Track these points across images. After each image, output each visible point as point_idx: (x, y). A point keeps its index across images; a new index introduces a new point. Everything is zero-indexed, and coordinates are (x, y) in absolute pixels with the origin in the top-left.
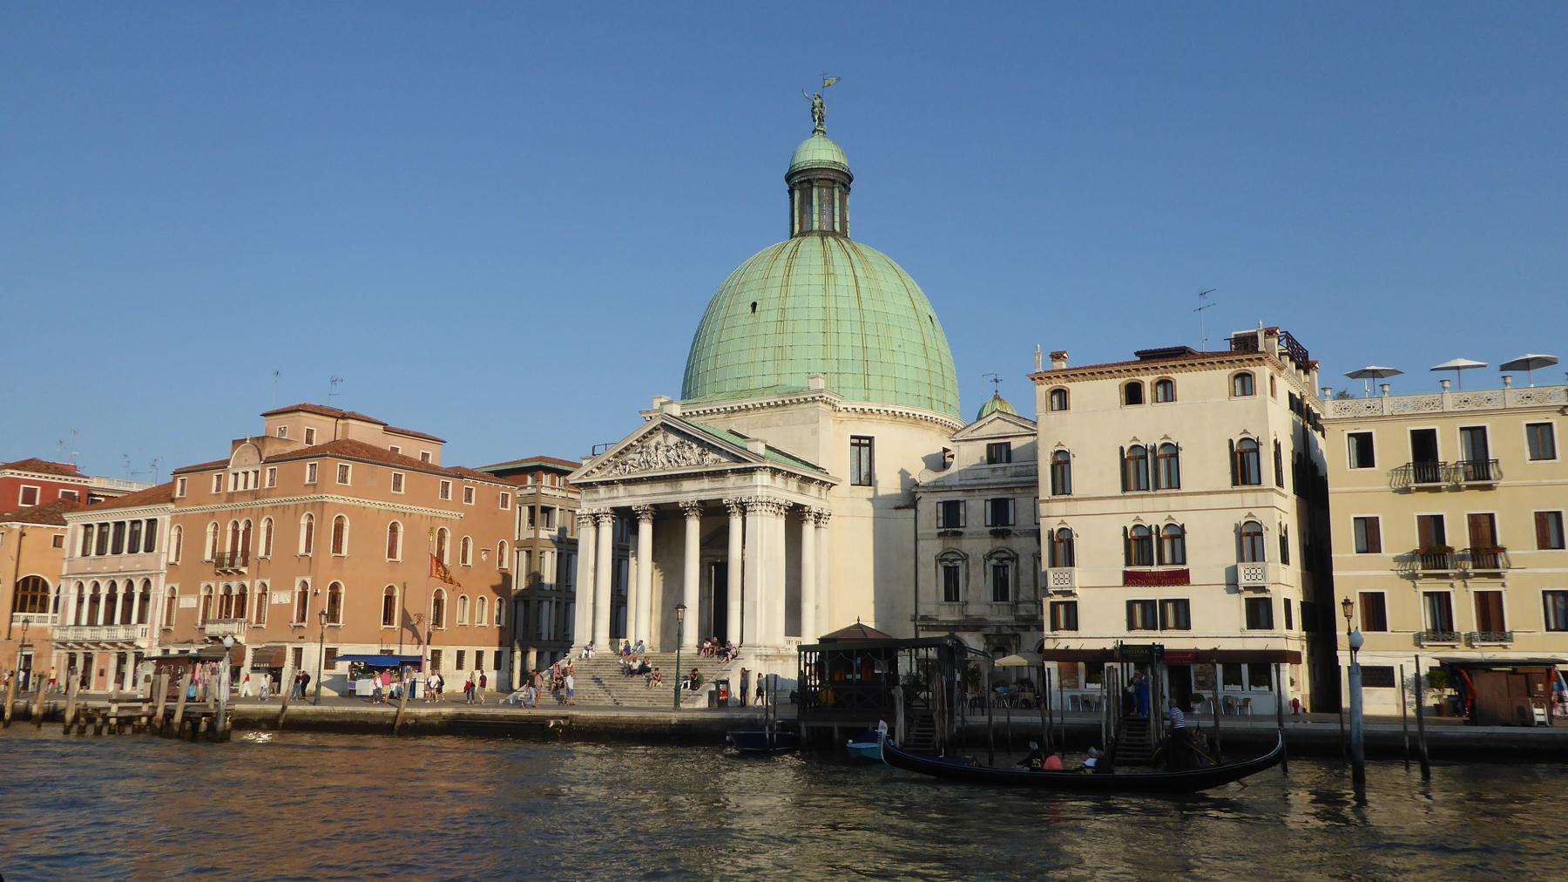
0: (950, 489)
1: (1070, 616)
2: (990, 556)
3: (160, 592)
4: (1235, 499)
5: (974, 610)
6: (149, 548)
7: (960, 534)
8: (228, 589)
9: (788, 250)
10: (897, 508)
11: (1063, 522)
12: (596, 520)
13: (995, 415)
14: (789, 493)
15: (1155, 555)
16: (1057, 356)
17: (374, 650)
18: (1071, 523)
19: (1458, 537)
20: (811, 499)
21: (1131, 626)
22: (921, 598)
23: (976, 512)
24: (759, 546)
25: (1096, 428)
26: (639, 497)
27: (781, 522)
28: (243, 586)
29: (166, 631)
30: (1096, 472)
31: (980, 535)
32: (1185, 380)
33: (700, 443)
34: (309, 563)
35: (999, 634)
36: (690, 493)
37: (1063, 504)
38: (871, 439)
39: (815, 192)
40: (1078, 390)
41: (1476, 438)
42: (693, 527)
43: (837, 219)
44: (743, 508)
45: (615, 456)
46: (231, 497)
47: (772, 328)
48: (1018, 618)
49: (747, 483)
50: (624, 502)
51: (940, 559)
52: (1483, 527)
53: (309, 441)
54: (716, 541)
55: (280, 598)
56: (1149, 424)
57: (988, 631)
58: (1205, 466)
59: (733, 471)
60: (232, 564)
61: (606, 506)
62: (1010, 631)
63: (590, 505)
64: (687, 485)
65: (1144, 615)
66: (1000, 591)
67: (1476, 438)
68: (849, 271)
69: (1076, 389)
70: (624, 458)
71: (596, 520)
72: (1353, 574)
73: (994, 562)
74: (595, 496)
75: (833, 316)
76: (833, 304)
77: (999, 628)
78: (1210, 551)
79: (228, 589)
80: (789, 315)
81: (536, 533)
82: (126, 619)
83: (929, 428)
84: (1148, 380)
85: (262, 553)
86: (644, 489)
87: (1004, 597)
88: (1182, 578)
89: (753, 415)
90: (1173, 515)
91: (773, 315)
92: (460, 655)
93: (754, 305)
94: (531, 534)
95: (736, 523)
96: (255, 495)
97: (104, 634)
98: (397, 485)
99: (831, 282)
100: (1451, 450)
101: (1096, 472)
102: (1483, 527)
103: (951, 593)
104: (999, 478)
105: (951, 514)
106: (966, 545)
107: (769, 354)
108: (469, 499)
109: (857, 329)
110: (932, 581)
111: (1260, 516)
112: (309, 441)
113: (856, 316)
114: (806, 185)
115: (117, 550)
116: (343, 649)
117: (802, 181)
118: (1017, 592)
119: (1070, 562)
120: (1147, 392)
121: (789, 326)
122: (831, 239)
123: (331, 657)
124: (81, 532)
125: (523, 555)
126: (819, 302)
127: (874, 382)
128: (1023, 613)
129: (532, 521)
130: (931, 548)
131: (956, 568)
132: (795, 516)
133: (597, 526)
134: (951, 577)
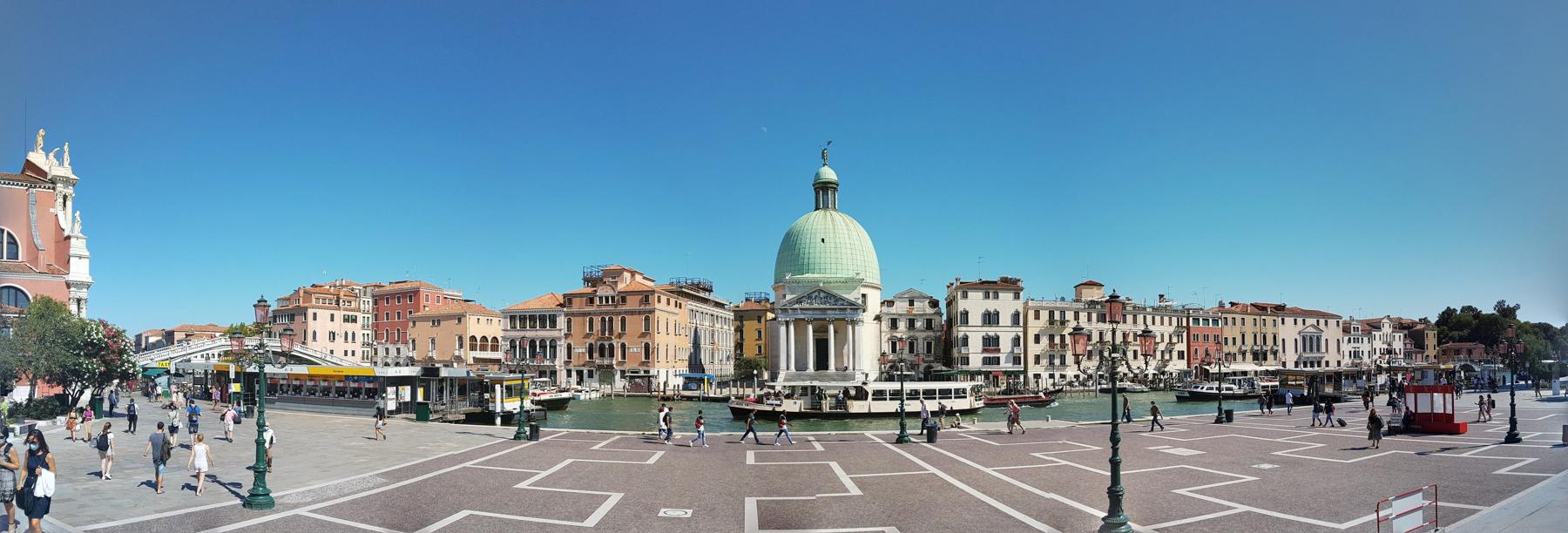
1: (966, 361)
12: (787, 323)
15: (991, 343)
30: (975, 318)
36: (831, 315)
56: (991, 305)
58: (1005, 319)
66: (911, 351)
71: (787, 323)
72: (1034, 349)
78: (1005, 345)
100: (1057, 316)
101: (975, 318)
105: (894, 324)
110: (887, 348)
117: (823, 188)
130: (885, 337)
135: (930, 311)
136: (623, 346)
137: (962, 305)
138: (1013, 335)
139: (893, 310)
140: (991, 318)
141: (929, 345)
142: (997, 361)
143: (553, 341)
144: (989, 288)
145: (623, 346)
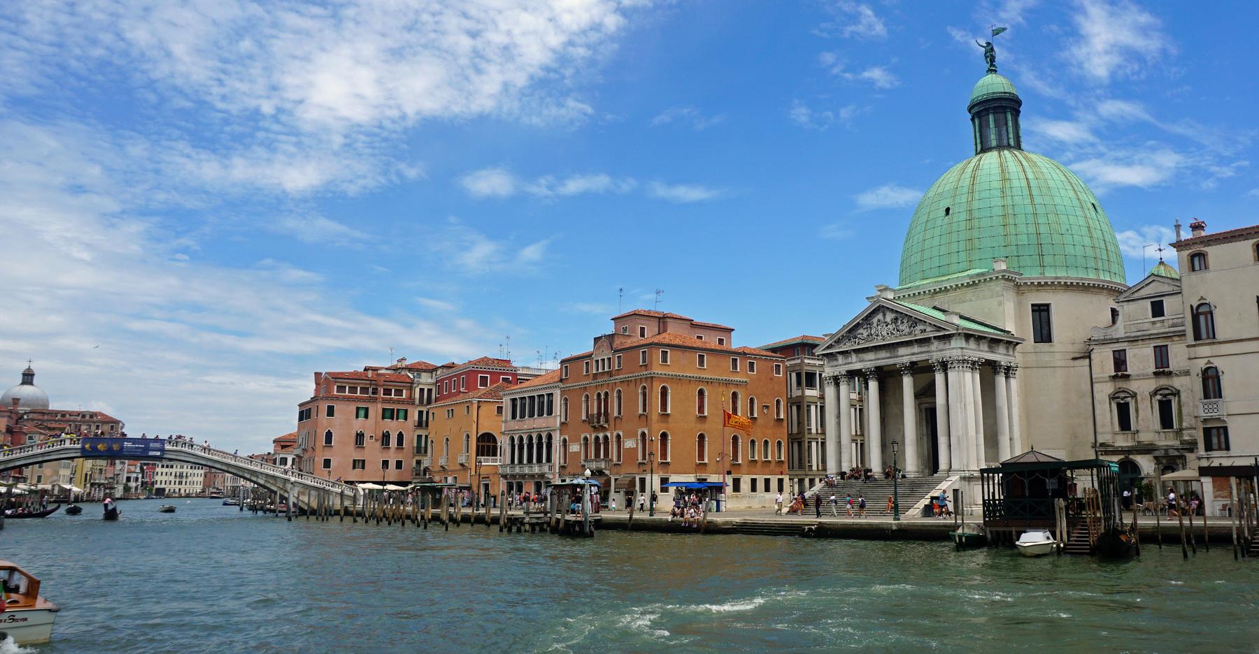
0: (1117, 341)
2: (1155, 393)
3: (557, 439)
5: (1145, 437)
6: (550, 413)
7: (1128, 376)
8: (597, 438)
9: (972, 165)
10: (1074, 359)
11: (1209, 362)
14: (982, 353)
16: (1197, 227)
17: (691, 478)
18: (1217, 362)
20: (1000, 356)
22: (1099, 429)
23: (1141, 359)
24: (961, 390)
27: (977, 376)
28: (606, 438)
29: (562, 467)
31: (1144, 377)
34: (644, 417)
35: (1166, 456)
36: (905, 356)
37: (1207, 348)
38: (1048, 305)
39: (991, 118)
40: (1212, 251)
42: (907, 381)
43: (1011, 136)
44: (944, 366)
45: (850, 331)
46: (595, 376)
49: (947, 346)
51: (1113, 397)
53: (642, 335)
54: (925, 393)
55: (629, 444)
57: (1157, 453)
60: (599, 422)
61: (843, 370)
62: (1176, 453)
64: (902, 351)
66: (1166, 421)
68: (1022, 176)
69: (1212, 251)
71: (836, 380)
73: (1159, 397)
75: (1011, 211)
76: (1010, 202)
77: (1166, 450)
79: (597, 438)
80: (976, 214)
81: (803, 392)
82: (539, 460)
83: (1098, 293)
85: (616, 414)
86: (871, 356)
87: (1172, 427)
89: (952, 294)
91: (963, 216)
92: (754, 481)
93: (948, 210)
94: (799, 393)
95: (939, 378)
96: (610, 374)
97: (527, 470)
98: (701, 363)
99: (1008, 185)
103: (1125, 424)
104: (1158, 329)
106: (1133, 386)
107: (962, 246)
108: (752, 369)
109: (1031, 219)
110: (1108, 416)
112: (642, 335)
113: (1030, 209)
115: (531, 415)
116: (674, 478)
121: (976, 223)
122: (1006, 152)
123: (664, 481)
124: (510, 403)
125: (794, 408)
127: (1048, 260)
128: (1186, 438)
129: (799, 383)
130: (1105, 390)
131: (1127, 404)
132: (989, 370)
133: (837, 385)
134: (1123, 411)
136: (618, 436)
139: (1120, 330)
143: (550, 437)
145: (618, 436)
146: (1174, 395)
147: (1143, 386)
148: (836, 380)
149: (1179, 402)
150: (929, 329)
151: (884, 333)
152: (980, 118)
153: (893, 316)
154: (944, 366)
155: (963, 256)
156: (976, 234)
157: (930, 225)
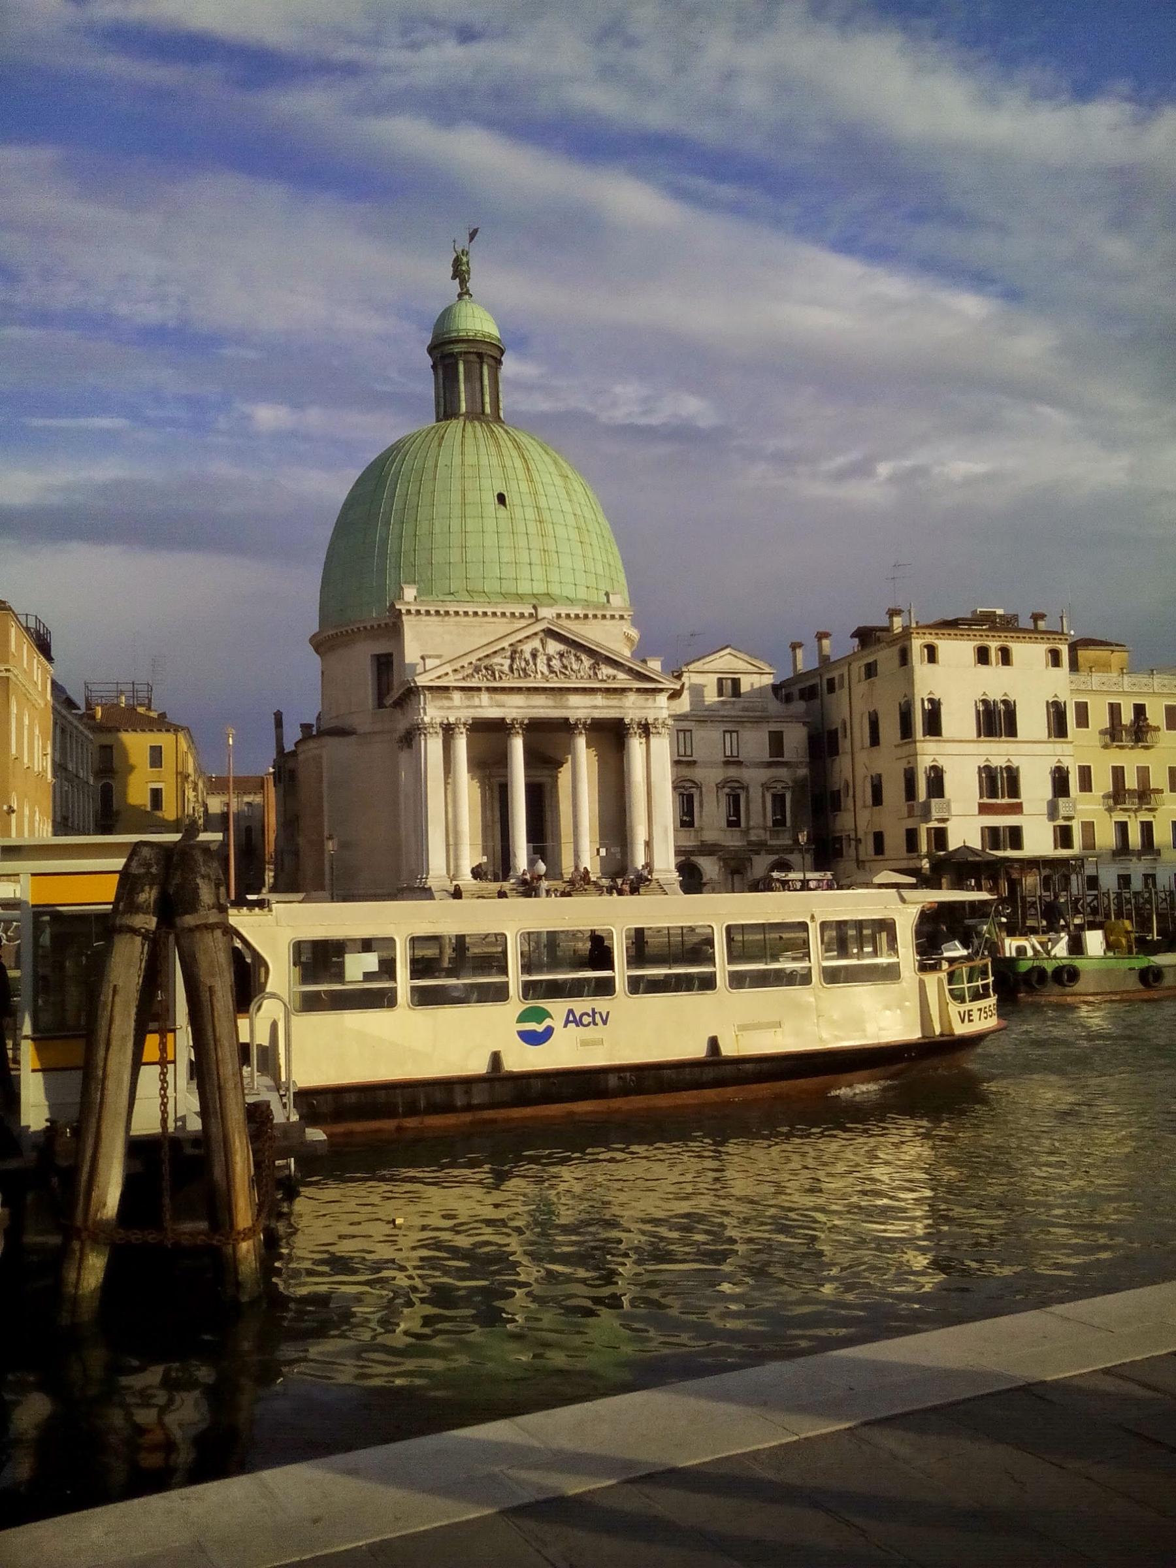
2: (720, 786)
4: (1049, 748)
5: (710, 836)
7: (695, 762)
13: (728, 650)
19: (1131, 782)
21: (1056, 848)
25: (952, 678)
26: (514, 708)
30: (959, 720)
32: (1018, 649)
33: (591, 653)
36: (580, 708)
39: (485, 368)
41: (1140, 710)
44: (646, 729)
45: (479, 659)
47: (532, 528)
48: (750, 843)
49: (650, 703)
50: (493, 713)
52: (1143, 773)
58: (1032, 720)
59: (639, 690)
61: (467, 715)
63: (443, 713)
64: (574, 700)
65: (993, 836)
67: (1140, 710)
70: (486, 662)
71: (448, 730)
73: (727, 790)
74: (446, 703)
80: (546, 515)
84: (993, 645)
86: (518, 700)
88: (1017, 809)
90: (1012, 758)
91: (530, 513)
93: (501, 499)
101: (959, 720)
102: (1143, 773)
106: (698, 774)
107: (536, 559)
111: (1067, 762)
114: (473, 358)
118: (748, 821)
119: (941, 794)
120: (994, 655)
126: (567, 507)
131: (690, 798)
135: (774, 706)
137: (928, 681)
138: (1053, 763)
140: (997, 720)
141: (779, 800)
142: (1015, 836)
144: (992, 631)
146: (742, 788)
147: (710, 776)
148: (448, 730)
149: (747, 797)
150: (621, 676)
151: (546, 670)
152: (465, 363)
153: (561, 647)
154: (646, 729)
155: (538, 572)
156: (552, 546)
157: (470, 511)
